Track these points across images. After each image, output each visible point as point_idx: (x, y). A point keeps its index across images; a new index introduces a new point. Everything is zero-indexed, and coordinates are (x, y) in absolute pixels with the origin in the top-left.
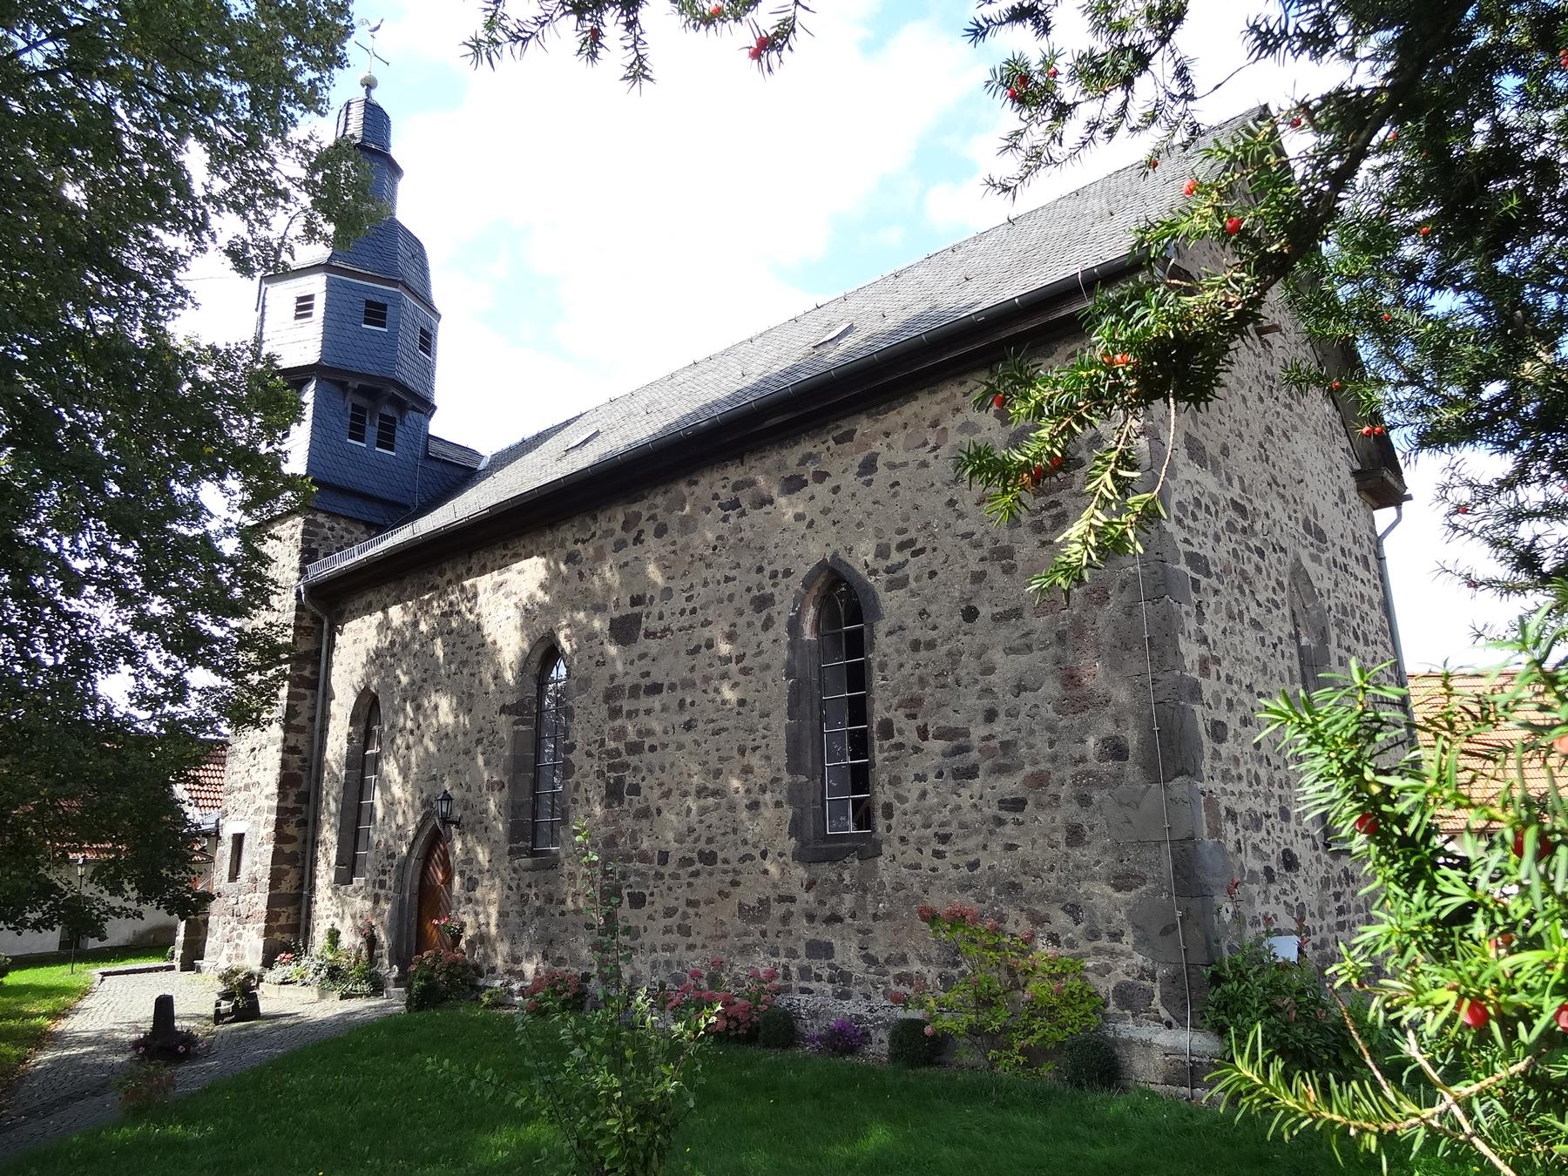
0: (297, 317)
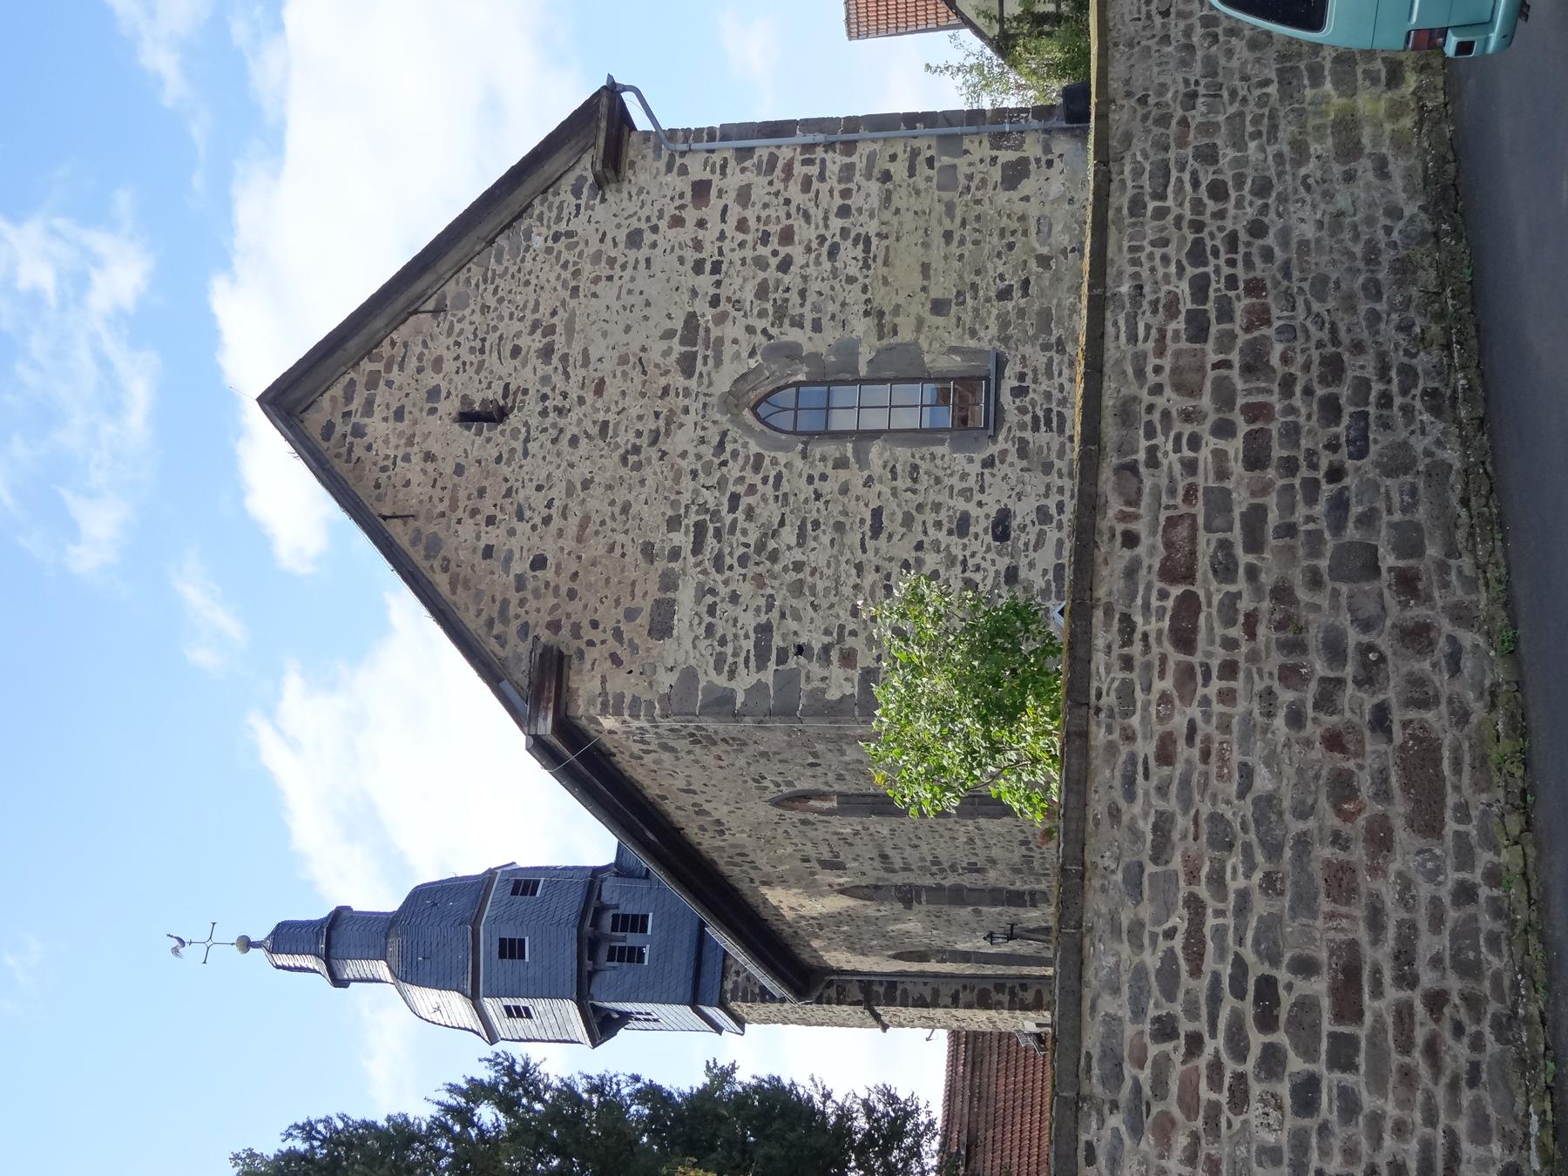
0: (529, 1016)
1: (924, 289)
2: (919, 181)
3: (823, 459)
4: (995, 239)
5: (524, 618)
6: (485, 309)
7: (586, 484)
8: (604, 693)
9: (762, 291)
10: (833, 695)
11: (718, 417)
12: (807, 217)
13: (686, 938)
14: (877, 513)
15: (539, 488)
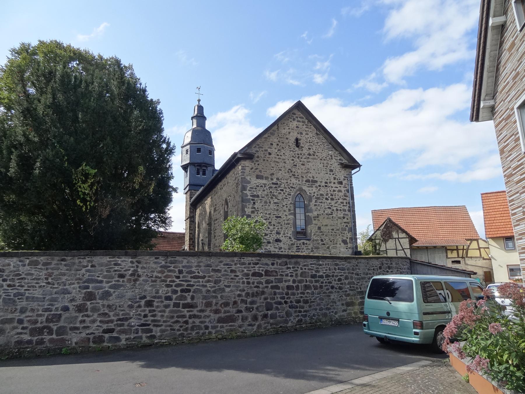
1: (323, 225)
2: (343, 224)
3: (290, 207)
4: (332, 238)
5: (259, 151)
6: (318, 143)
7: (285, 162)
8: (245, 166)
9: (322, 195)
10: (246, 209)
11: (298, 187)
12: (336, 203)
13: (201, 183)
14: (280, 217)
15: (284, 154)
